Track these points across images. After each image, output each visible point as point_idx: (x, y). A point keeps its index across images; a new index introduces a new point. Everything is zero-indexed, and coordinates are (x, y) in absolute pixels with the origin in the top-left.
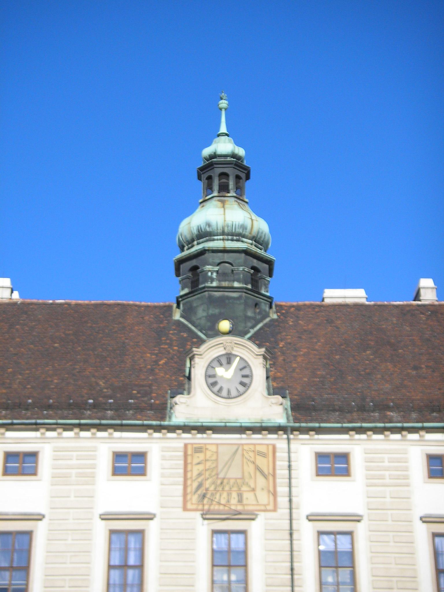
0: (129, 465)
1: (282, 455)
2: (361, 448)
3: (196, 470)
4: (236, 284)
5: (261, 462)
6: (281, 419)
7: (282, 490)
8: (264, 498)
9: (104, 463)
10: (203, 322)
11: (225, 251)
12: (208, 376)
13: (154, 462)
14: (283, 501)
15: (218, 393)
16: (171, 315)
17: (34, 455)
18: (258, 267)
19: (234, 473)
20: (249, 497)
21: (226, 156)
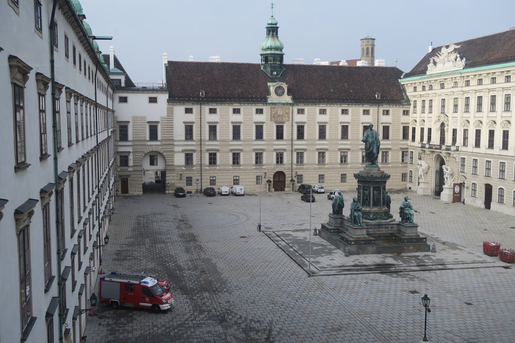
0: (260, 111)
1: (291, 110)
2: (307, 109)
3: (273, 113)
4: (277, 63)
5: (287, 111)
6: (291, 102)
7: (291, 117)
8: (287, 118)
9: (254, 111)
10: (269, 72)
11: (275, 54)
12: (275, 91)
13: (265, 111)
14: (291, 119)
15: (277, 95)
16: (260, 68)
17: (239, 109)
18: (281, 56)
19: (281, 113)
20: (284, 118)
21: (273, 24)
